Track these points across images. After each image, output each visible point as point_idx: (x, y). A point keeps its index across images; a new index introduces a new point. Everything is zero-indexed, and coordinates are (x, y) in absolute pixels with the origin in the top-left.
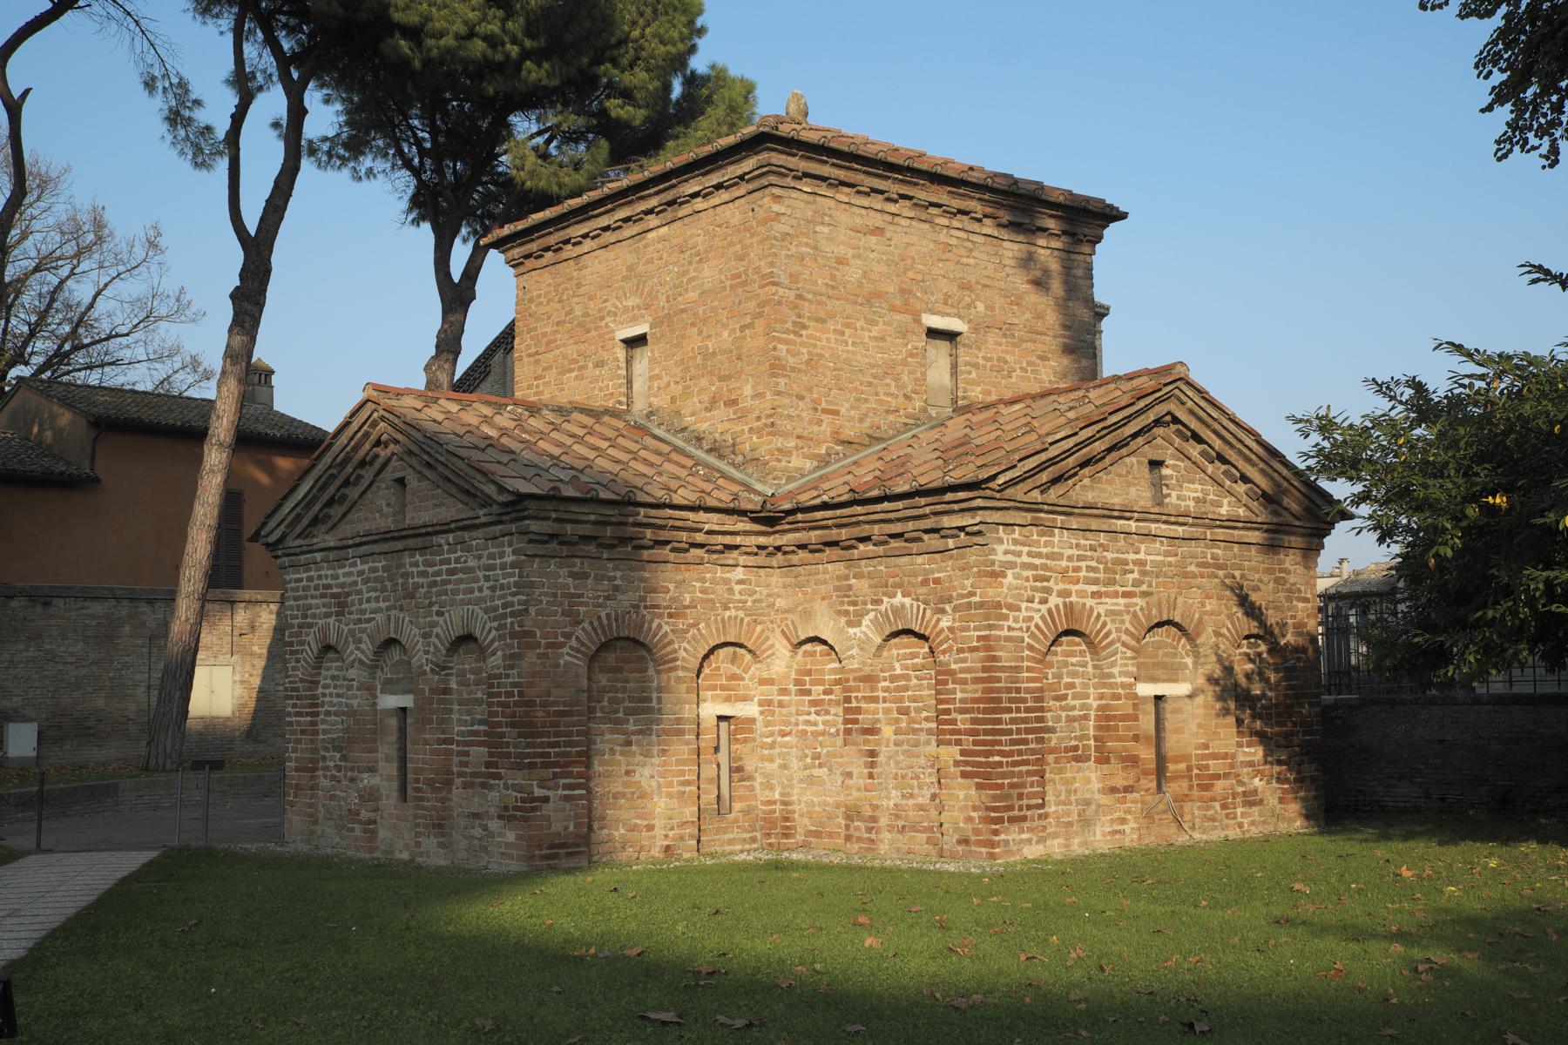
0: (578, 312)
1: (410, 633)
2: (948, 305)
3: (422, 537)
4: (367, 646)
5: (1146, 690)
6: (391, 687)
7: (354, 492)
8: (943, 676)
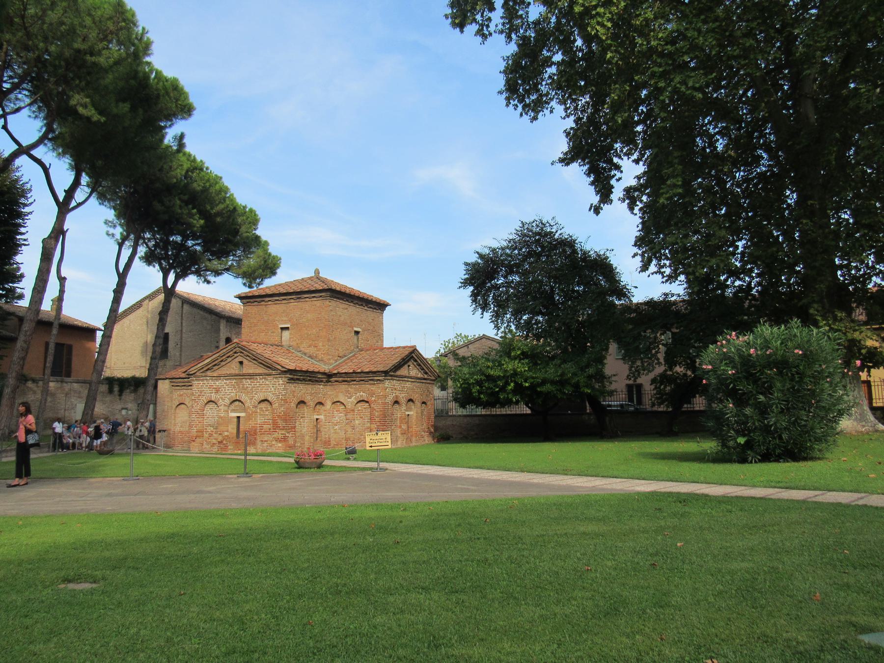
0: (266, 318)
1: (244, 398)
2: (358, 325)
3: (251, 376)
4: (227, 402)
5: (407, 413)
6: (234, 411)
7: (223, 363)
8: (372, 410)
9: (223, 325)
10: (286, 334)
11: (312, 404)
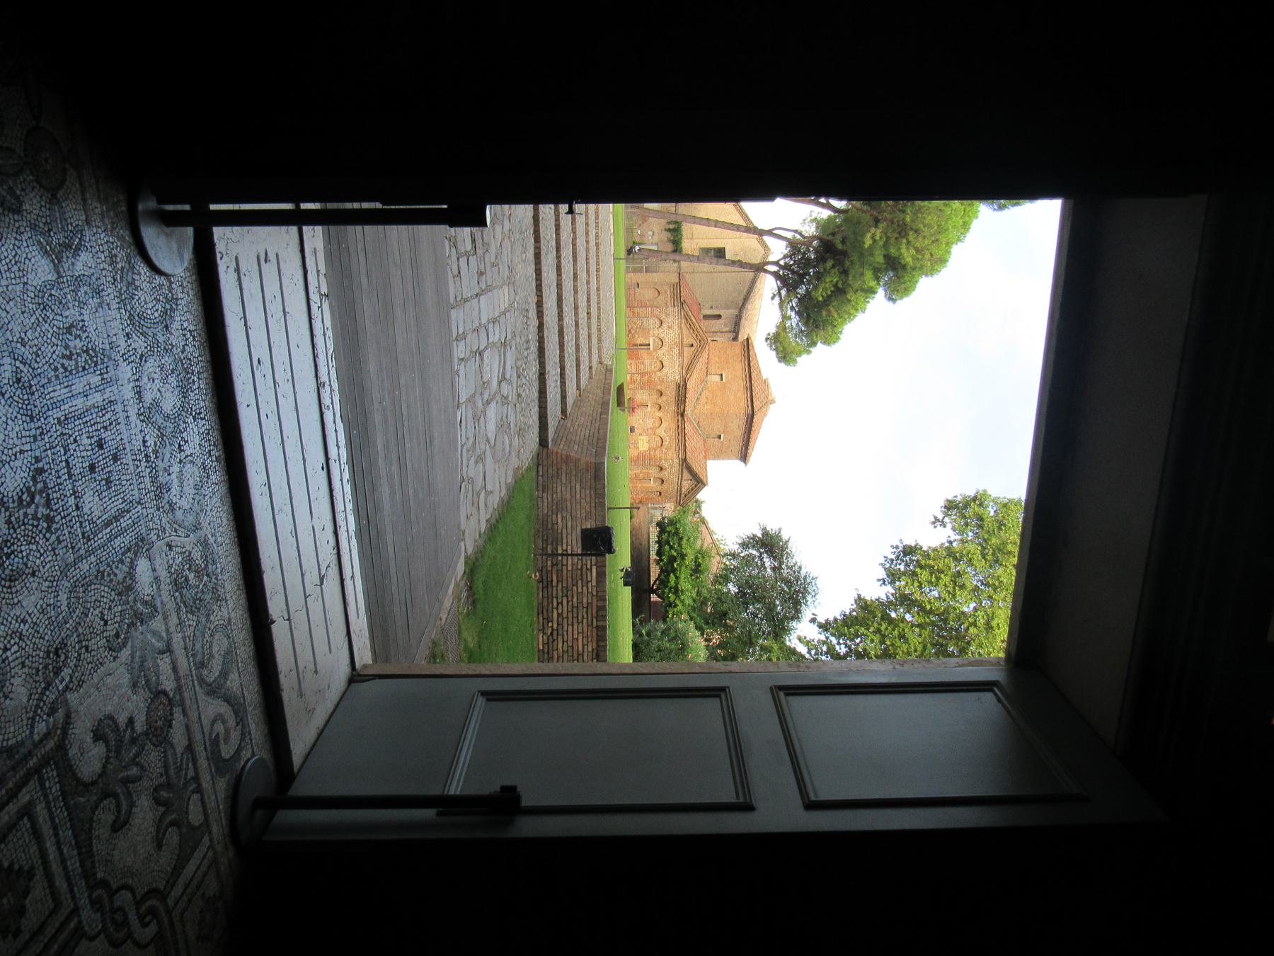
3: (681, 354)
9: (735, 312)
10: (718, 378)
11: (660, 401)
